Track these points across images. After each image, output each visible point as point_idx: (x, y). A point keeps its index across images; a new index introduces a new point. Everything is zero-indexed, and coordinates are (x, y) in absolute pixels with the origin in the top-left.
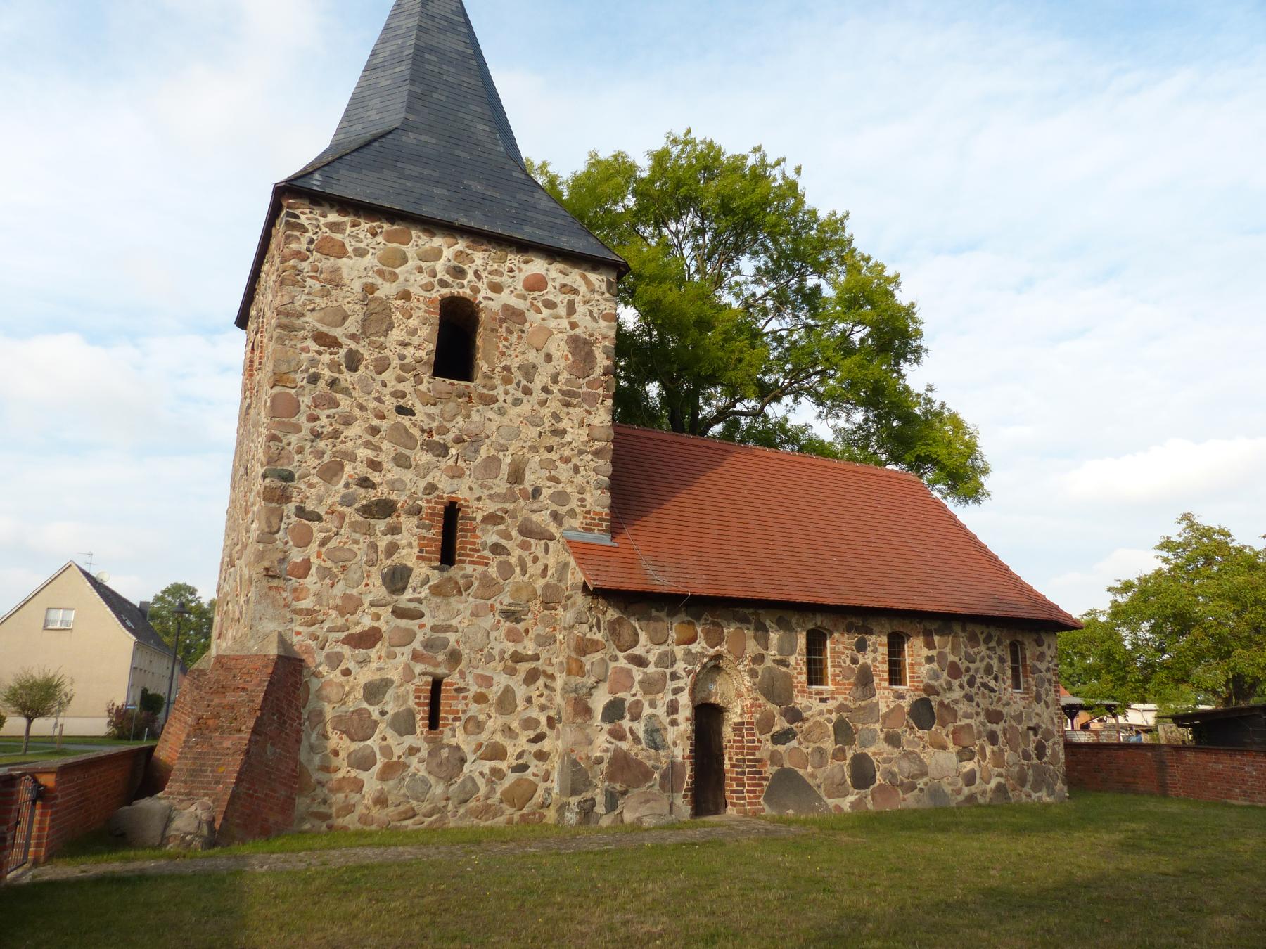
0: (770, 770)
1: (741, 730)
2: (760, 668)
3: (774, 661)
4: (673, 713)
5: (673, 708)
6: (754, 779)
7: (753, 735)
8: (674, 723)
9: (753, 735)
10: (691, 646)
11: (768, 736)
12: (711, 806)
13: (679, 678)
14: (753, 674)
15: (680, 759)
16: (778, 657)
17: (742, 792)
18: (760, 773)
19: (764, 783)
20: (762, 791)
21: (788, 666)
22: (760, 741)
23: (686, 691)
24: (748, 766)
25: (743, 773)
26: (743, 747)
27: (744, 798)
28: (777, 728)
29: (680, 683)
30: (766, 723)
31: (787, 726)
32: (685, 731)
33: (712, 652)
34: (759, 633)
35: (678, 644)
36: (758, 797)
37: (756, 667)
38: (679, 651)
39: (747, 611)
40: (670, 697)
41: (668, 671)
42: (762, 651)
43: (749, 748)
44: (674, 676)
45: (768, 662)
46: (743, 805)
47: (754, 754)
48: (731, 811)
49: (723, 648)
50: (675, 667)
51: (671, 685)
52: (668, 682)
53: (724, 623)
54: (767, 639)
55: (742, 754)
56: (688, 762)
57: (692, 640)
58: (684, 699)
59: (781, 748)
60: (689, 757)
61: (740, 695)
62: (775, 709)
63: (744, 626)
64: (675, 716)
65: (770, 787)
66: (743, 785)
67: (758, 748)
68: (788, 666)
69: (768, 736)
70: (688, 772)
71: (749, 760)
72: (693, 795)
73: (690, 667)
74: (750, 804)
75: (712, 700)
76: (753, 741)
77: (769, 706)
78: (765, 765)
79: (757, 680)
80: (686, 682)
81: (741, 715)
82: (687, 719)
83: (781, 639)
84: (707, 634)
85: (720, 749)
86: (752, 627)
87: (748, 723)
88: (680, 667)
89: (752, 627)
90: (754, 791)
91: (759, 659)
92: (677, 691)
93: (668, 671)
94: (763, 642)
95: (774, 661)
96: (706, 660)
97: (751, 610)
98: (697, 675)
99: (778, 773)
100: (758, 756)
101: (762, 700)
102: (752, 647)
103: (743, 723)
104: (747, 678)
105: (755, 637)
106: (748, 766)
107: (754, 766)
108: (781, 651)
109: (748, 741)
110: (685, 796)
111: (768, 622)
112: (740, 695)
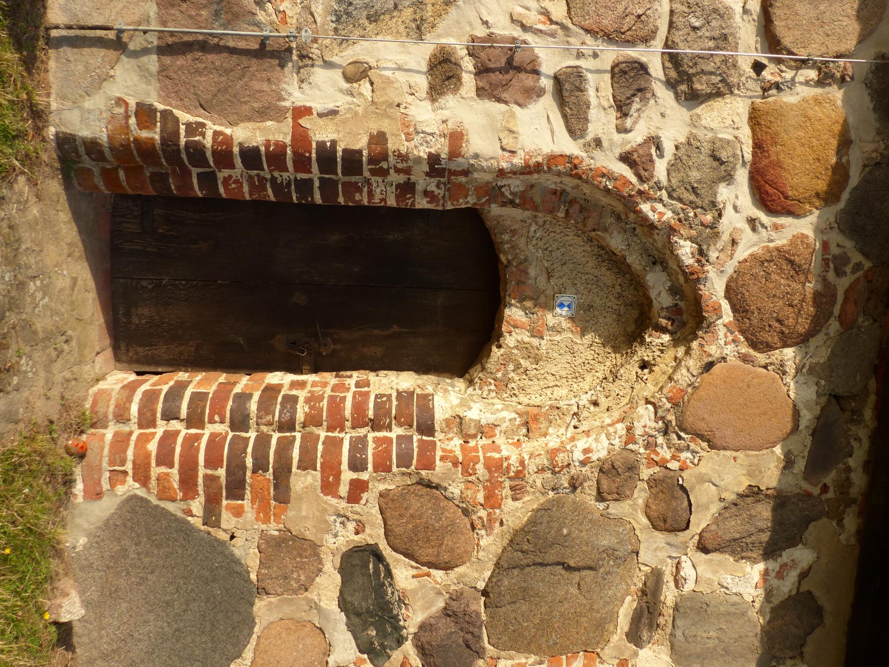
0: (244, 531)
1: (404, 420)
2: (633, 510)
3: (656, 576)
4: (482, 71)
5: (503, 70)
6: (213, 462)
7: (383, 466)
8: (443, 72)
9: (383, 466)
10: (742, 176)
11: (375, 535)
12: (144, 313)
13: (622, 108)
14: (615, 476)
15: (295, 94)
16: (669, 595)
17: (170, 415)
18: (236, 488)
19: (197, 506)
20: (165, 493)
21: (634, 637)
22: (358, 489)
23: (569, 146)
24: (263, 441)
25: (239, 422)
26: (337, 424)
27: (147, 421)
28: (404, 574)
29: (601, 121)
30: (423, 526)
31: (412, 619)
32: (411, 130)
33: (715, 288)
34: (764, 512)
35: (755, 118)
36: (142, 477)
37: (641, 495)
38: (727, 120)
39: (855, 461)
40: (551, 59)
41: (652, 57)
42: (700, 522)
43: (333, 445)
44: (630, 80)
45: (654, 549)
46: (122, 417)
47: (307, 464)
48: (118, 379)
49: (723, 341)
50: (664, 95)
51: (598, 61)
52: (611, 54)
53: (820, 350)
54: (737, 547)
55: (313, 420)
56: (279, 132)
57: (769, 196)
58: (536, 132)
59: (328, 586)
60: (301, 137)
61: (530, 423)
62: (476, 573)
63: (803, 443)
64: (468, 80)
65: (186, 530)
66: (195, 420)
67: (329, 487)
68: (634, 637)
69: (375, 535)
70: (245, 134)
71: (285, 446)
72: (146, 150)
73: (660, 169)
74: (121, 441)
75: (514, 313)
76: (357, 465)
77: (490, 544)
78: (264, 513)
79: (587, 496)
80: (604, 145)
81: (458, 423)
82: (456, 138)
83: (736, 610)
84: (787, 260)
85: (338, 365)
86: (797, 483)
87: (428, 449)
88: (665, 120)
89: (797, 483)
90: (165, 458)
91: (671, 512)
92: (568, 91)
93: (652, 57)
94: (733, 528)
95: (656, 576)
96: (686, 250)
97: (859, 480)
98: (629, 203)
99: (233, 568)
100: (303, 482)
101: (515, 512)
102: (721, 477)
103: (427, 428)
104: (600, 452)
105: (754, 493)
106: (263, 441)
107: (260, 465)
108: (694, 608)
109: (358, 445)
110: (145, 113)
111: (802, 555)
112: (530, 423)
